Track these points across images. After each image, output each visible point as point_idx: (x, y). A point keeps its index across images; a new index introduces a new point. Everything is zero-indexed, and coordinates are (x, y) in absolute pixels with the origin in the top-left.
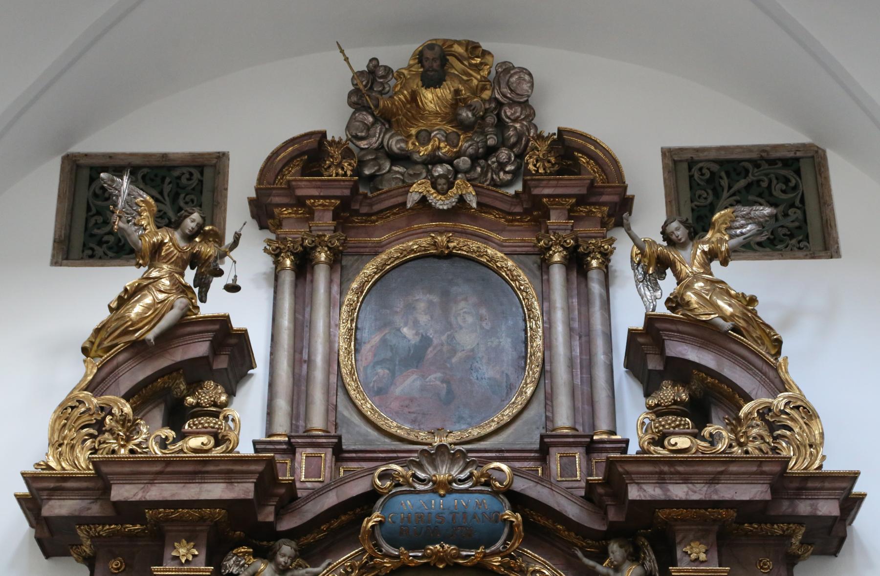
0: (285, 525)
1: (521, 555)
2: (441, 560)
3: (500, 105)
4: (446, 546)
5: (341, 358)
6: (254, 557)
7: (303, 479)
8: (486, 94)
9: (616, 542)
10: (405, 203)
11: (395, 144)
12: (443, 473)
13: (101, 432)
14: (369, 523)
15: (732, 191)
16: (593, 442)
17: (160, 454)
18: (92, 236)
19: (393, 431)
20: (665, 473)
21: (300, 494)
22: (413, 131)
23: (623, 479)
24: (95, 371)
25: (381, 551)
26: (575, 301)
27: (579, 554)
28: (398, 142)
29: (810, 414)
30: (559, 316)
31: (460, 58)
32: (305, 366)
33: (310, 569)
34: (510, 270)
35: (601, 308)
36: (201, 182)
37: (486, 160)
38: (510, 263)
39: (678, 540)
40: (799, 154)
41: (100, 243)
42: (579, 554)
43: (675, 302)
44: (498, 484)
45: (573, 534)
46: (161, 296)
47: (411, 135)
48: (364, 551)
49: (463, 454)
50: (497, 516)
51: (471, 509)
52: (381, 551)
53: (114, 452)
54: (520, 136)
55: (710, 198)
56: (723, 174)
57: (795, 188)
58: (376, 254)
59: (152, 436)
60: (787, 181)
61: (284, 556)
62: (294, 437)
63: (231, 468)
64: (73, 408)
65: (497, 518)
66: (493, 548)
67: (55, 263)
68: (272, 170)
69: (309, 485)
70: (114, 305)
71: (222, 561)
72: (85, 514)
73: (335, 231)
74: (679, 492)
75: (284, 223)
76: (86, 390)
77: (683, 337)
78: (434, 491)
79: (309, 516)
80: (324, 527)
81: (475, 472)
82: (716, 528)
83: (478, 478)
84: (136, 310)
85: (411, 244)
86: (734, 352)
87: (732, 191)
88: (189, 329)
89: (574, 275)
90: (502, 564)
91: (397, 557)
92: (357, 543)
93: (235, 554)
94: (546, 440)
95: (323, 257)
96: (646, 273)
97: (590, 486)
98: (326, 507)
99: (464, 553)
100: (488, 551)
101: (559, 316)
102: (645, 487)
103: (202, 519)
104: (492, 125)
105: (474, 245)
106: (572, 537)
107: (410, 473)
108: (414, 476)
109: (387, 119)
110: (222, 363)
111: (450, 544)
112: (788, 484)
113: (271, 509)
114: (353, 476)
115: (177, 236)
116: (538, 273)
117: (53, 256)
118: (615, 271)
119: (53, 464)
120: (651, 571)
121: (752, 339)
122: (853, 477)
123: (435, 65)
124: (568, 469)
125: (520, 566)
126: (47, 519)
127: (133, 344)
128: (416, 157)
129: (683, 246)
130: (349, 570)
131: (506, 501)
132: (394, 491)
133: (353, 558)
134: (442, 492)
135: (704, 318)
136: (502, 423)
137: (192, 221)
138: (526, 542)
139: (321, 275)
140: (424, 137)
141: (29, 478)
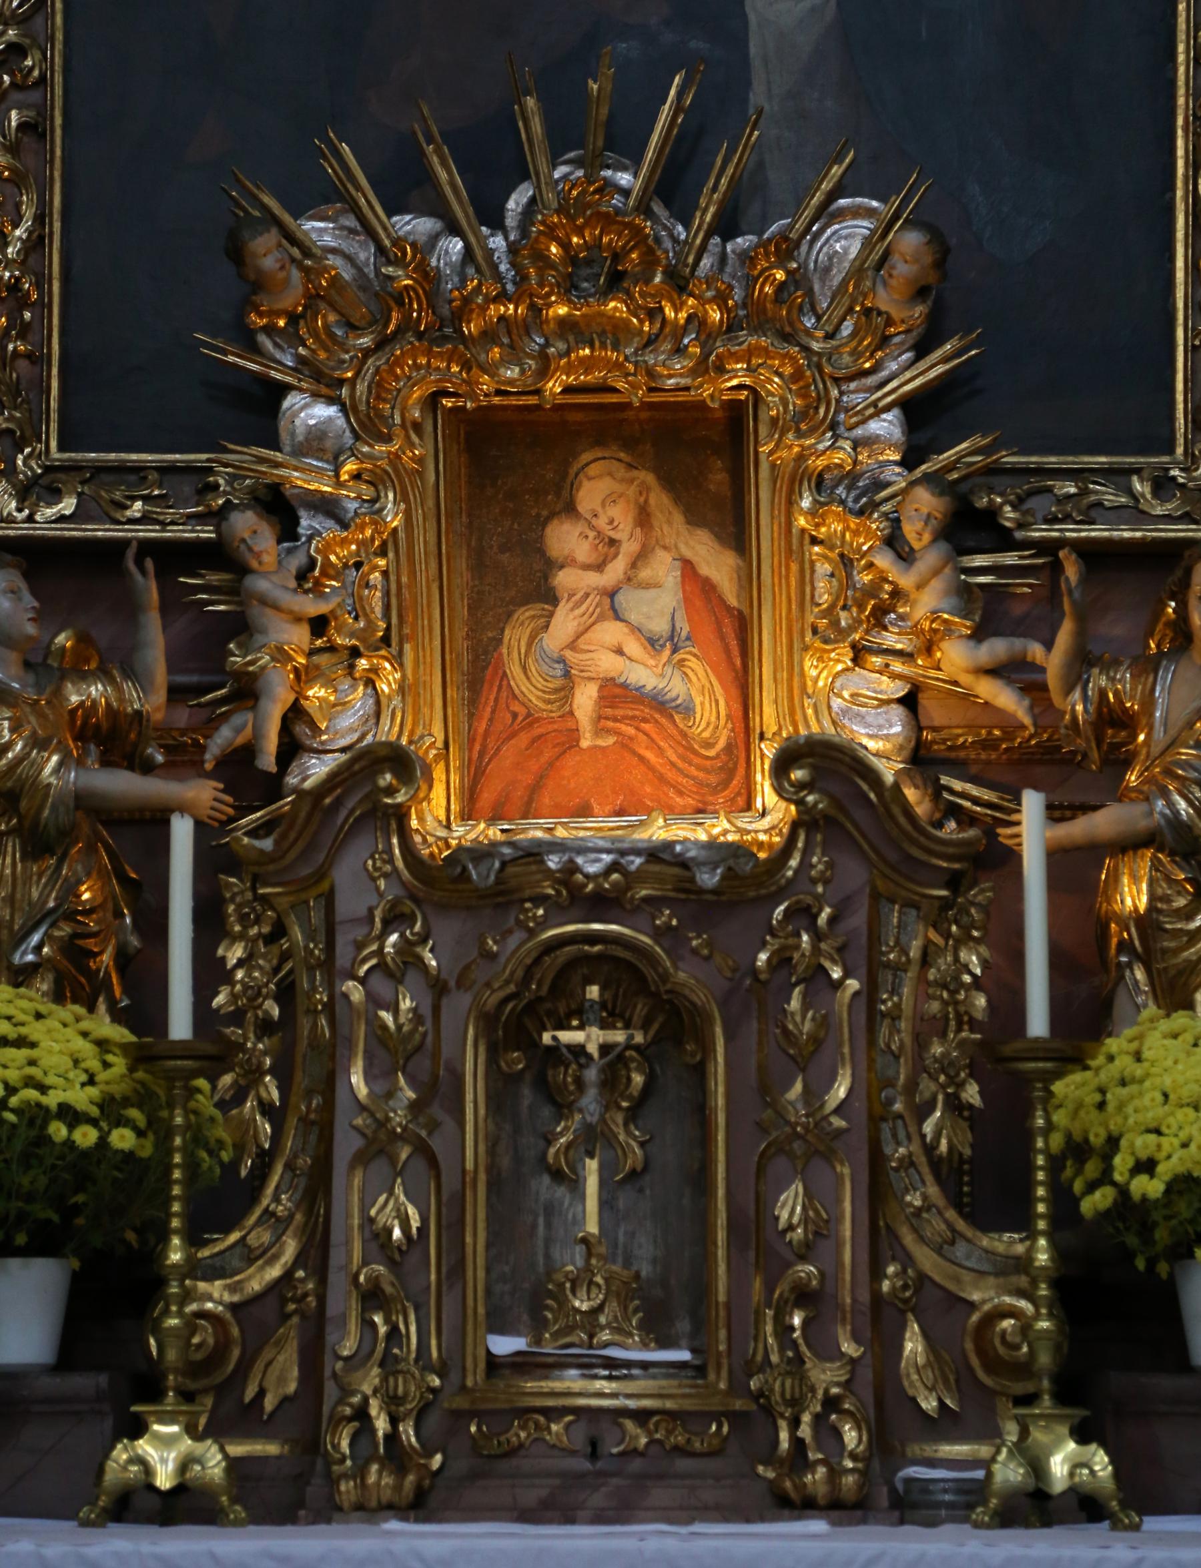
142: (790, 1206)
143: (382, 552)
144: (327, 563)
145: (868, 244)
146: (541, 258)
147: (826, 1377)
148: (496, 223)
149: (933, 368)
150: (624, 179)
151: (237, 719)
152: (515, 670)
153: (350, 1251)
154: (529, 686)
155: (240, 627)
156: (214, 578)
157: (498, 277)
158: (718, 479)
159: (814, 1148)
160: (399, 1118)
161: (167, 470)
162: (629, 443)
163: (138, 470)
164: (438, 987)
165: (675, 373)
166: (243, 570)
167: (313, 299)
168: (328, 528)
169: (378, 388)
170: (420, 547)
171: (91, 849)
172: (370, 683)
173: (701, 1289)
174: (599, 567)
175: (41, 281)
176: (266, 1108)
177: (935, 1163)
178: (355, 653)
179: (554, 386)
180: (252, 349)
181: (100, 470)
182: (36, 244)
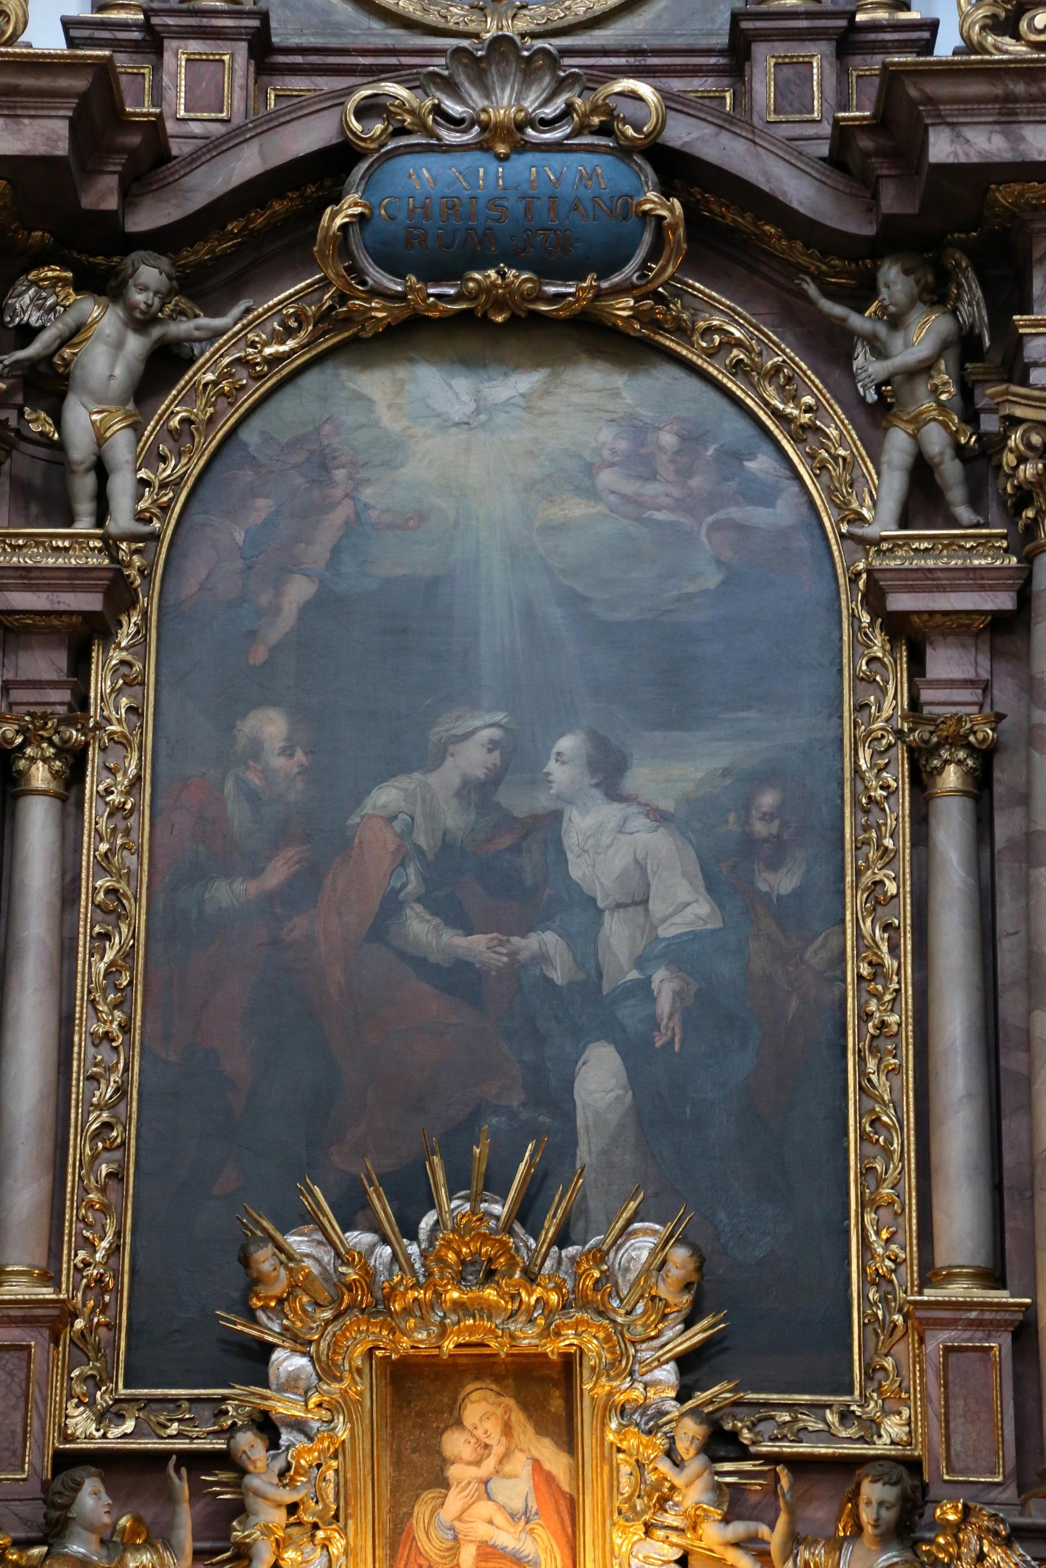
1: (680, 294)
2: (500, 304)
4: (511, 273)
6: (77, 291)
7: (182, 113)
9: (896, 262)
12: (504, 104)
14: (336, 218)
16: (854, 27)
20: (1015, 99)
23: (919, 116)
25: (364, 283)
27: (812, 290)
33: (204, 321)
42: (812, 290)
44: (630, 131)
45: (799, 245)
48: (325, 283)
49: (553, 60)
50: (626, 205)
51: (567, 190)
52: (364, 283)
61: (144, 289)
62: (157, 12)
66: (616, 279)
69: (196, 128)
78: (483, 146)
79: (199, 201)
80: (232, 227)
81: (578, 101)
83: (586, 116)
90: (637, 315)
91: (401, 297)
92: (310, 264)
93: (33, 283)
94: (745, 25)
97: (842, 134)
98: (236, 180)
99: (551, 290)
100: (605, 285)
102: (969, 133)
106: (798, 252)
107: (429, 103)
108: (438, 110)
111: (521, 267)
113: (110, 182)
114: (297, 109)
120: (972, 326)
124: (792, 93)
125: (678, 319)
130: (293, 324)
131: (649, 169)
132: (391, 145)
133: (300, 297)
134: (502, 149)
138: (692, 264)
143: (335, 1456)
144: (299, 1465)
145: (653, 1253)
146: (441, 1261)
148: (413, 1237)
149: (696, 1336)
150: (497, 1209)
152: (420, 1535)
155: (239, 1510)
156: (224, 1476)
157: (414, 1273)
158: (556, 1404)
161: (193, 1400)
162: (498, 1379)
163: (175, 1400)
165: (528, 1338)
166: (243, 1472)
167: (293, 1287)
168: (300, 1441)
169: (335, 1345)
170: (359, 1454)
172: (325, 1547)
174: (478, 1463)
175: (117, 1275)
178: (315, 1527)
179: (449, 1345)
180: (251, 1317)
181: (151, 1400)
182: (115, 1250)
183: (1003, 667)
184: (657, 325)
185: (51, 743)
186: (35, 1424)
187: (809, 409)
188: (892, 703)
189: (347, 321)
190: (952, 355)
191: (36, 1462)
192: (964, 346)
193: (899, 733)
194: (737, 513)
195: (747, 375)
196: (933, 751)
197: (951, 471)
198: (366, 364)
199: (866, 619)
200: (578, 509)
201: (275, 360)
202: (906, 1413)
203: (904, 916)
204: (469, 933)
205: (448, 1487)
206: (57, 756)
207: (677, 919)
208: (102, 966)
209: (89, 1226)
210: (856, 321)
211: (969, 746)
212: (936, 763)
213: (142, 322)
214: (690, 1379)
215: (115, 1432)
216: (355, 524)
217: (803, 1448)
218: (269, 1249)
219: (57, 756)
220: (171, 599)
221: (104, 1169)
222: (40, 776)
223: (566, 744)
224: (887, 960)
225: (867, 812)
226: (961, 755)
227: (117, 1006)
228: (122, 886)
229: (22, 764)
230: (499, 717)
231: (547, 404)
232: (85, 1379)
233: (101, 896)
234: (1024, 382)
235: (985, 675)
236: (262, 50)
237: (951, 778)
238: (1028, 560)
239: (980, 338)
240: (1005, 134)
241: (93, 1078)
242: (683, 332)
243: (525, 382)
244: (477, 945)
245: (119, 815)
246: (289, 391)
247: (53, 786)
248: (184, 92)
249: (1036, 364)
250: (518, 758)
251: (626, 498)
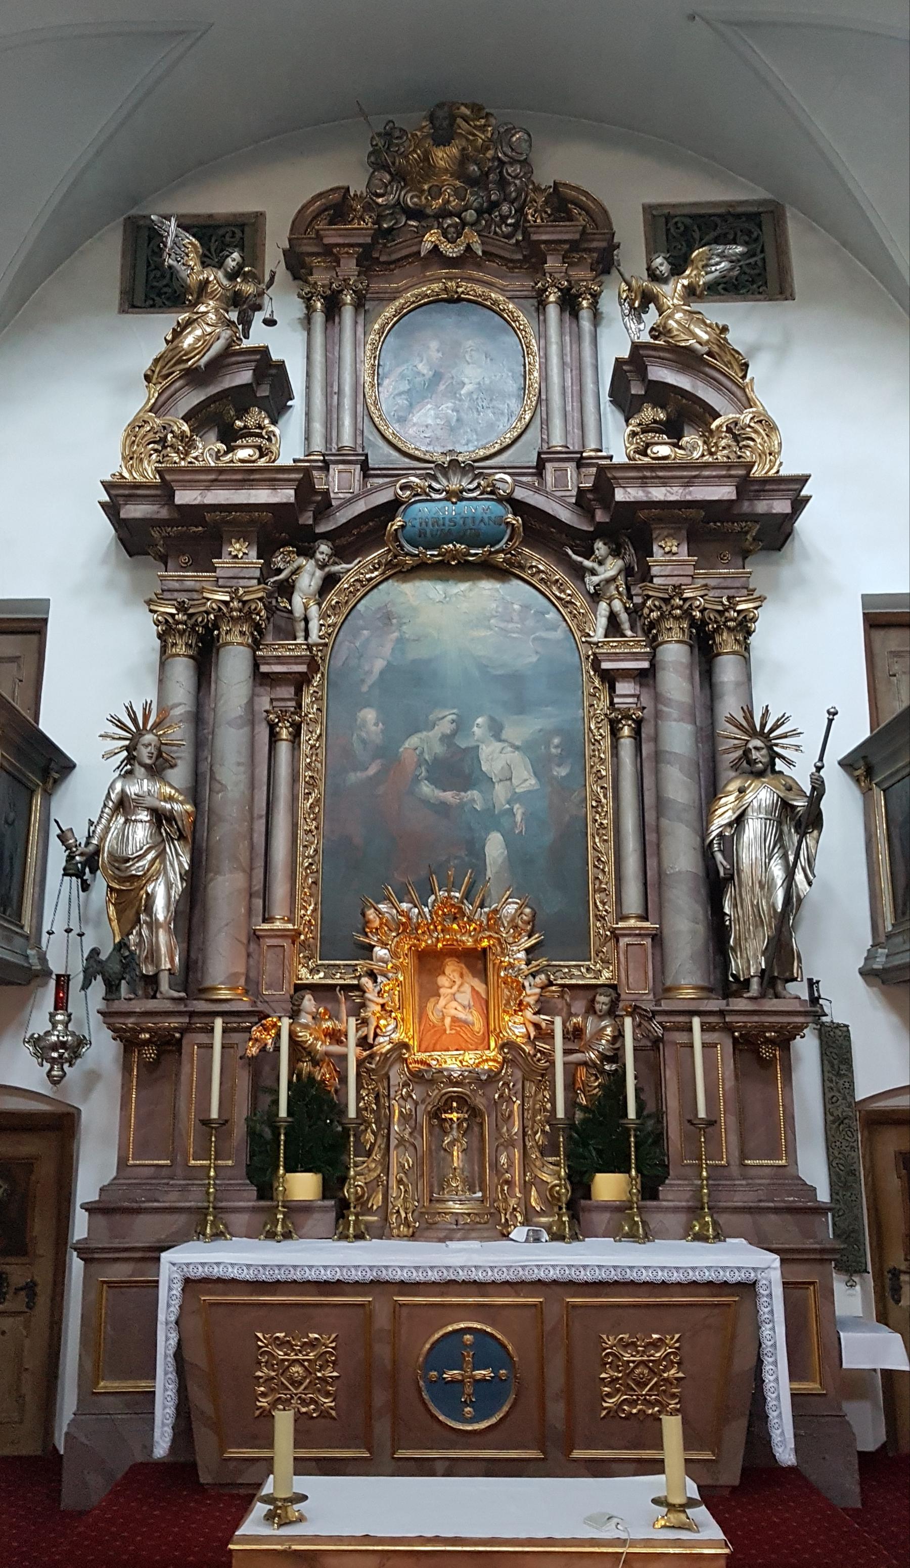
0: (321, 529)
1: (520, 553)
3: (502, 163)
4: (458, 546)
5: (367, 390)
6: (298, 555)
7: (336, 490)
8: (490, 154)
10: (419, 252)
11: (410, 201)
12: (454, 485)
13: (164, 447)
15: (703, 242)
16: (582, 458)
17: (213, 464)
18: (153, 287)
19: (411, 452)
20: (646, 478)
21: (334, 503)
22: (426, 187)
24: (156, 395)
25: (403, 550)
26: (567, 338)
27: (570, 552)
28: (412, 198)
29: (770, 427)
30: (554, 349)
31: (465, 119)
32: (336, 397)
33: (344, 566)
34: (512, 312)
35: (591, 343)
36: (242, 239)
37: (490, 215)
38: (511, 306)
39: (654, 536)
40: (761, 210)
41: (159, 295)
42: (570, 552)
43: (656, 332)
44: (502, 492)
45: (564, 536)
46: (209, 330)
47: (424, 190)
48: (389, 551)
52: (403, 550)
53: (175, 463)
54: (519, 191)
55: (684, 249)
56: (695, 228)
57: (756, 240)
58: (395, 299)
59: (207, 450)
60: (749, 233)
62: (328, 455)
63: (272, 476)
64: (140, 427)
65: (501, 521)
66: (497, 547)
67: (123, 311)
68: (302, 225)
69: (341, 495)
70: (169, 338)
71: (271, 557)
72: (155, 516)
73: (358, 276)
74: (658, 494)
75: (314, 271)
76: (150, 411)
77: (664, 362)
78: (446, 499)
81: (482, 482)
82: (687, 525)
83: (484, 488)
84: (188, 341)
85: (424, 289)
86: (707, 375)
87: (703, 242)
88: (234, 359)
89: (567, 315)
92: (384, 544)
93: (282, 553)
94: (543, 456)
95: (348, 299)
96: (632, 307)
97: (581, 492)
99: (472, 551)
101: (554, 349)
102: (629, 490)
103: (252, 521)
104: (494, 182)
105: (479, 289)
107: (427, 484)
108: (430, 486)
109: (400, 177)
110: (264, 391)
112: (750, 487)
114: (380, 488)
115: (220, 274)
116: (535, 315)
117: (121, 305)
118: (602, 313)
119: (126, 475)
121: (721, 363)
122: (803, 480)
123: (445, 124)
124: (560, 482)
125: (519, 563)
126: (124, 520)
127: (188, 372)
128: (428, 211)
129: (665, 281)
130: (377, 566)
131: (508, 506)
133: (380, 556)
134: (454, 500)
135: (683, 344)
136: (504, 445)
137: (233, 259)
138: (524, 543)
139: (348, 313)
140: (435, 192)
141: (108, 486)
142: (503, 1159)
145: (516, 910)
146: (436, 913)
147: (513, 1202)
149: (533, 941)
150: (457, 895)
151: (363, 1029)
152: (430, 1014)
153: (394, 1168)
154: (434, 1018)
155: (363, 1005)
156: (357, 993)
157: (426, 918)
158: (480, 965)
159: (511, 1143)
160: (407, 1136)
161: (344, 965)
162: (457, 957)
163: (339, 966)
164: (416, 1103)
165: (470, 943)
166: (364, 992)
167: (381, 924)
168: (385, 981)
169: (397, 946)
171: (328, 1065)
173: (482, 1181)
176: (373, 1132)
177: (538, 1147)
178: (391, 1011)
179: (440, 945)
180: (367, 936)
183: (645, 690)
184: (512, 565)
185: (288, 721)
186: (287, 974)
187: (569, 595)
188: (602, 705)
189: (396, 566)
190: (623, 574)
191: (288, 989)
192: (628, 571)
193: (606, 715)
194: (544, 634)
195: (546, 583)
196: (619, 721)
197: (624, 617)
198: (405, 581)
199: (592, 673)
200: (483, 633)
201: (371, 579)
202: (611, 968)
203: (608, 784)
204: (445, 791)
205: (440, 996)
206: (290, 726)
207: (523, 785)
208: (308, 805)
209: (305, 901)
210: (587, 563)
211: (633, 719)
212: (620, 726)
213: (322, 567)
214: (530, 957)
215: (316, 977)
216: (400, 640)
217: (573, 982)
218: (372, 910)
219: (290, 726)
220: (331, 669)
221: (310, 881)
222: (284, 734)
223: (480, 720)
224: (603, 800)
225: (594, 744)
226: (630, 722)
227: (314, 820)
228: (315, 775)
229: (278, 729)
230: (455, 711)
231: (471, 594)
232: (304, 957)
233: (307, 779)
234: (651, 582)
235: (638, 693)
236: (365, 466)
237: (626, 731)
238: (654, 649)
239: (633, 568)
240: (644, 491)
241: (305, 846)
242: (522, 567)
243: (464, 586)
244: (448, 796)
245: (314, 749)
246: (375, 590)
247: (289, 737)
248: (338, 482)
249: (656, 576)
250: (461, 725)
251: (502, 629)
